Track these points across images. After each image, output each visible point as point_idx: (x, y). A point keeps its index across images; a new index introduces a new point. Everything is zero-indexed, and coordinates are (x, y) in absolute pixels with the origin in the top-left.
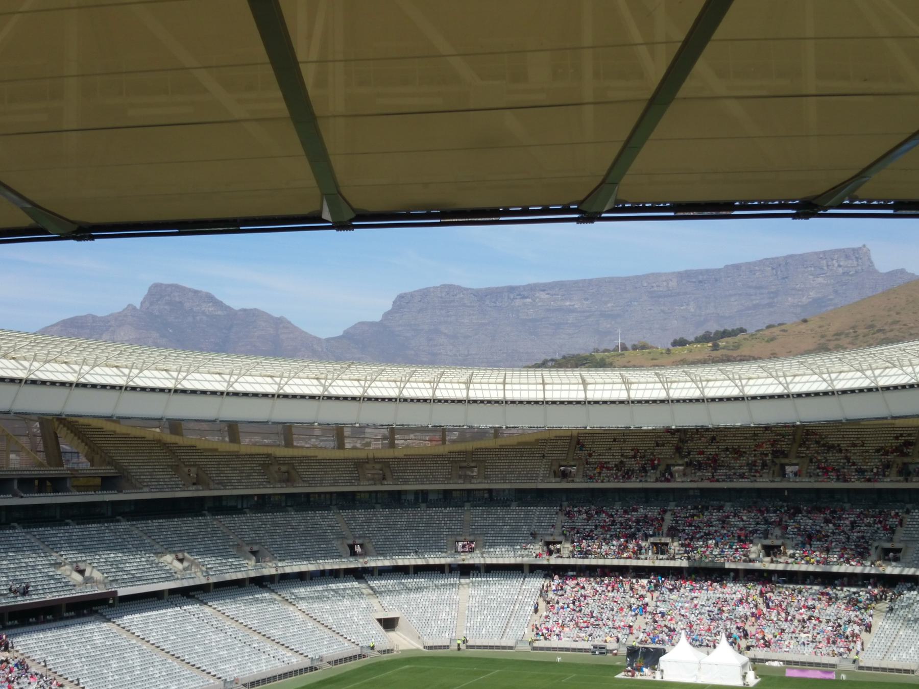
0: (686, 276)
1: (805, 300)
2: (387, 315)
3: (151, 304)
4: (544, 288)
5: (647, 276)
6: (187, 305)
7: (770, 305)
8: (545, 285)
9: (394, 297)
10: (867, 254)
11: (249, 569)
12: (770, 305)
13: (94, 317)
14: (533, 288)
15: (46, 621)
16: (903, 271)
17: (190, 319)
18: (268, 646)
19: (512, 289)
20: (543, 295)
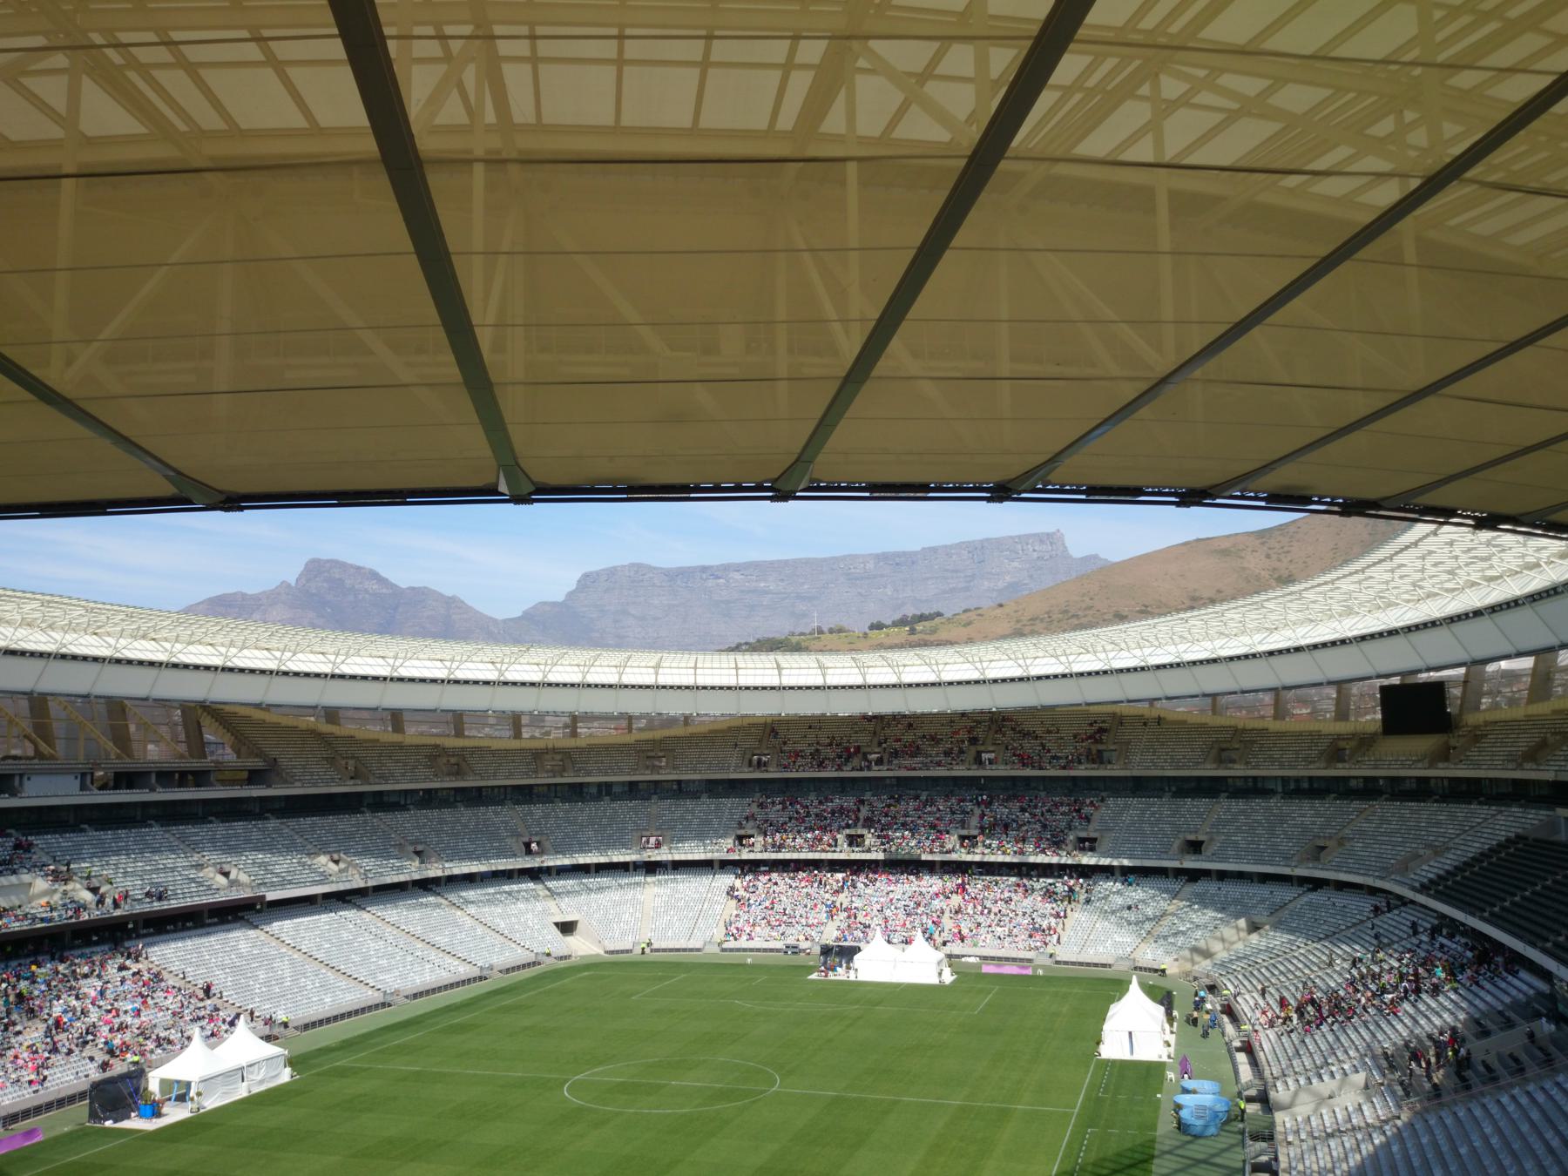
0: (884, 558)
1: (1001, 584)
2: (570, 595)
3: (308, 581)
4: (738, 568)
5: (844, 558)
6: (348, 583)
7: (967, 589)
8: (739, 565)
9: (578, 576)
10: (1062, 538)
11: (412, 870)
12: (967, 589)
13: (244, 595)
14: (727, 568)
15: (185, 928)
16: (1096, 557)
17: (351, 598)
18: (433, 955)
19: (704, 569)
20: (737, 576)
